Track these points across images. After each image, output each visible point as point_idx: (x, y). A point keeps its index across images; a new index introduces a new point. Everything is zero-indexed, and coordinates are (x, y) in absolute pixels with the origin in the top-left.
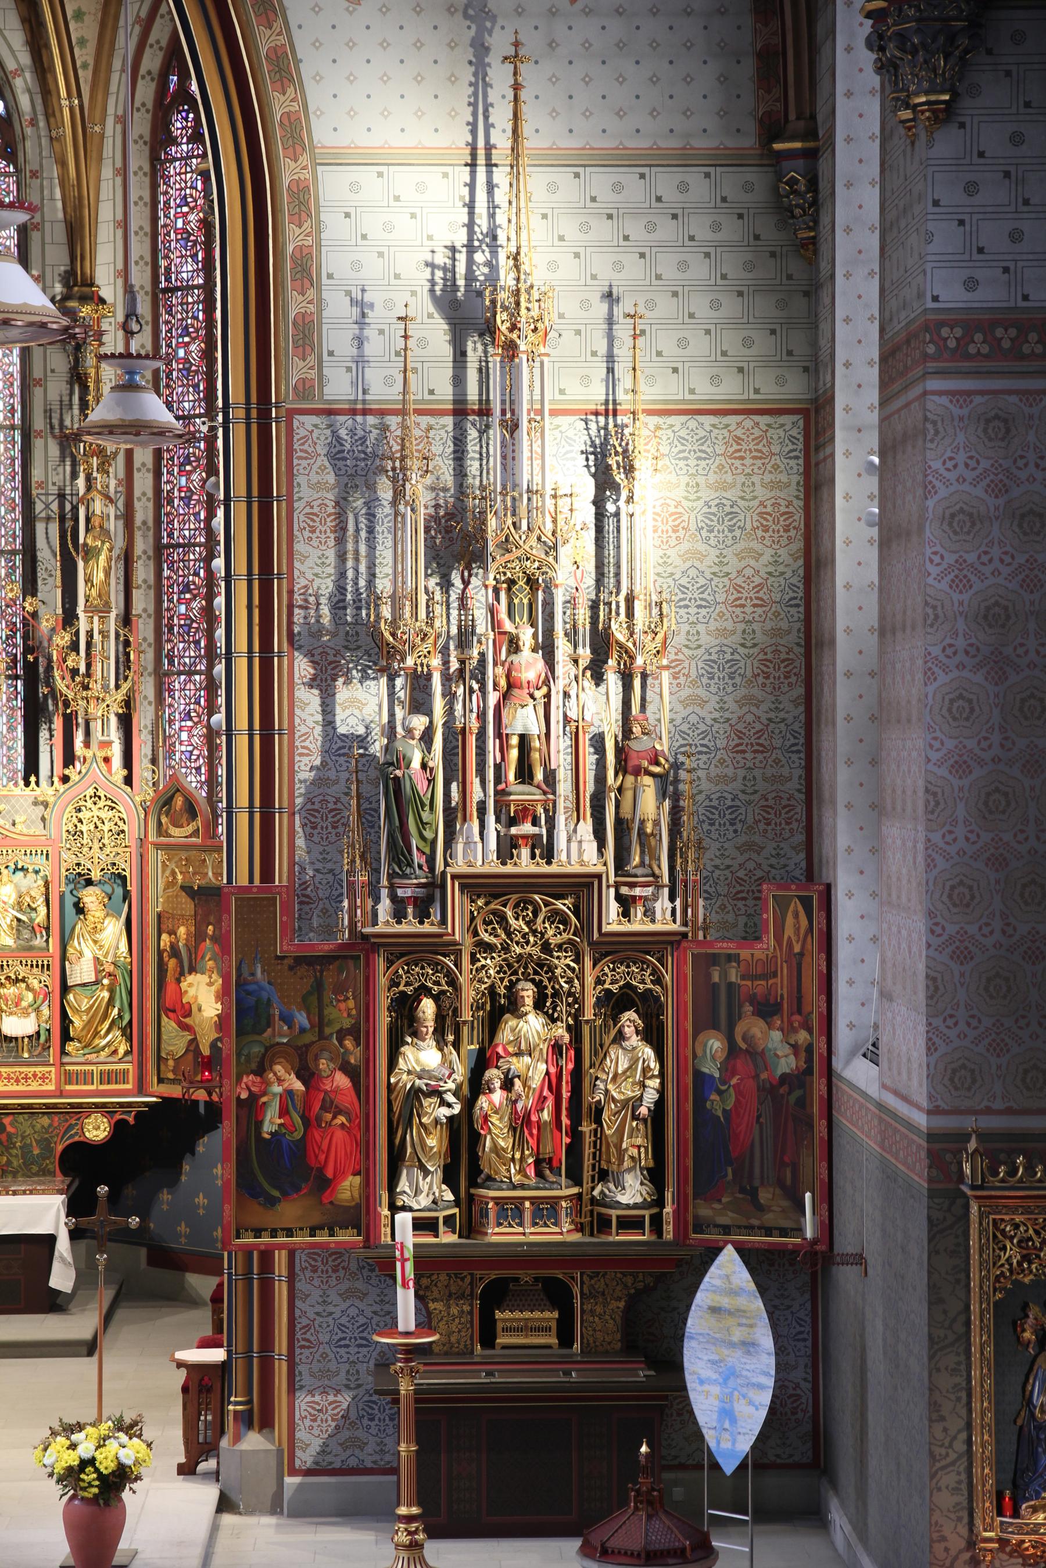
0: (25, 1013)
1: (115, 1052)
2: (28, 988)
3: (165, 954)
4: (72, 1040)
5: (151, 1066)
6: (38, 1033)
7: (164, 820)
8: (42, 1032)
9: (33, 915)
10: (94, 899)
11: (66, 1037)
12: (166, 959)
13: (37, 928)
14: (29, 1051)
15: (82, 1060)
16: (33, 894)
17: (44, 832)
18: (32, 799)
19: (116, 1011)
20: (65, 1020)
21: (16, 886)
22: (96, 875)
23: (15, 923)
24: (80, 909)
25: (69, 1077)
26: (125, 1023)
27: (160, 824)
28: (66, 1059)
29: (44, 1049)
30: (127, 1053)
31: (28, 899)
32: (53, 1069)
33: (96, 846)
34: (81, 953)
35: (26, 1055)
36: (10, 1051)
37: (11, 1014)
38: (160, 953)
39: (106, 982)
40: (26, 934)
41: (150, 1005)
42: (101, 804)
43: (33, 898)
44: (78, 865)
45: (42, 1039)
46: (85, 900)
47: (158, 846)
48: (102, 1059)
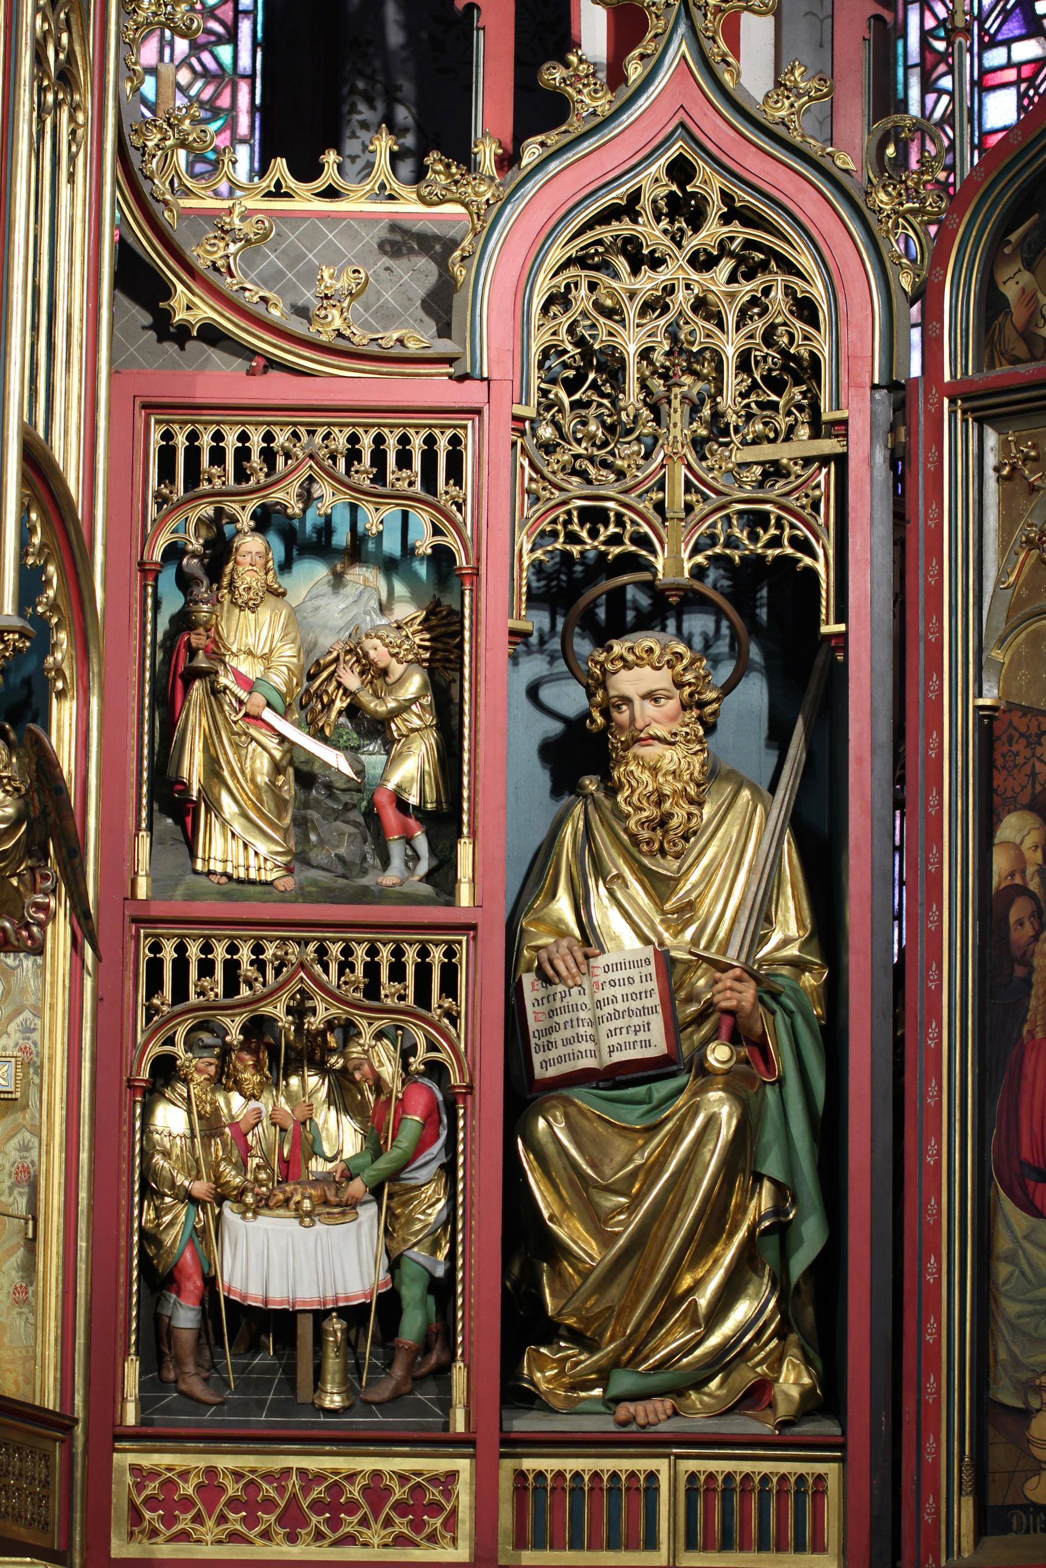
0: (333, 1202)
1: (758, 1395)
2: (345, 1092)
3: (1019, 910)
4: (548, 1331)
5: (943, 1446)
6: (390, 1303)
7: (1014, 284)
8: (412, 1293)
9: (374, 759)
10: (661, 680)
11: (526, 1323)
12: (1021, 933)
13: (390, 816)
14: (349, 1389)
15: (604, 1424)
16: (378, 653)
17: (445, 347)
18: (380, 231)
19: (765, 1199)
20: (526, 1240)
21: (297, 622)
22: (673, 561)
23: (287, 784)
24: (581, 755)
25: (543, 1511)
26: (800, 1262)
27: (992, 304)
28: (525, 1423)
29: (418, 1381)
30: (812, 1406)
31: (352, 681)
32: (463, 1466)
33: (679, 428)
34: (589, 938)
35: (333, 1400)
36: (252, 1383)
37: (263, 1204)
38: (991, 907)
39: (719, 1055)
40: (342, 840)
41: (948, 1151)
42: (712, 232)
43: (376, 675)
44: (594, 517)
45: (412, 1324)
46: (628, 683)
47: (984, 406)
48: (697, 1423)
